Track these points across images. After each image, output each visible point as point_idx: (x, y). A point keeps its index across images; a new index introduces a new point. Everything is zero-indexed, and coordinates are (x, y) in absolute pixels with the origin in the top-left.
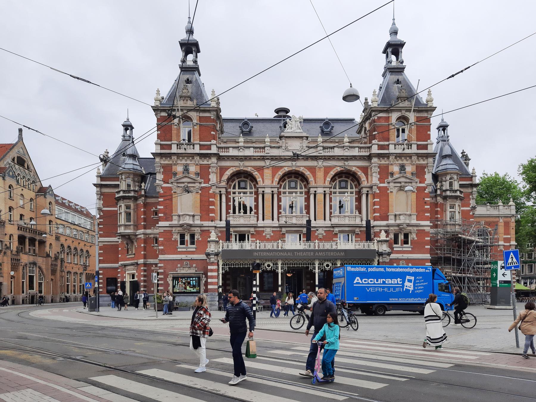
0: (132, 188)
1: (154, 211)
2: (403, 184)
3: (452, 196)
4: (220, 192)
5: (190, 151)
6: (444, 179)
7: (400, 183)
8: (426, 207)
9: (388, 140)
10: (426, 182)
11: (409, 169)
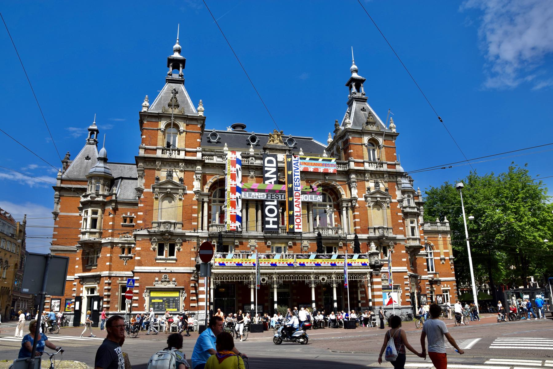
0: (101, 193)
1: (123, 217)
2: (379, 199)
4: (203, 199)
5: (175, 155)
7: (376, 198)
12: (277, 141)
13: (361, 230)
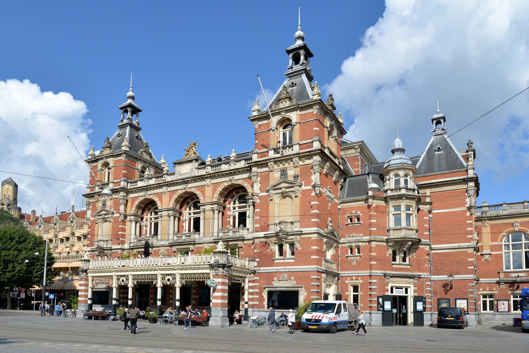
7: (280, 189)
13: (260, 228)
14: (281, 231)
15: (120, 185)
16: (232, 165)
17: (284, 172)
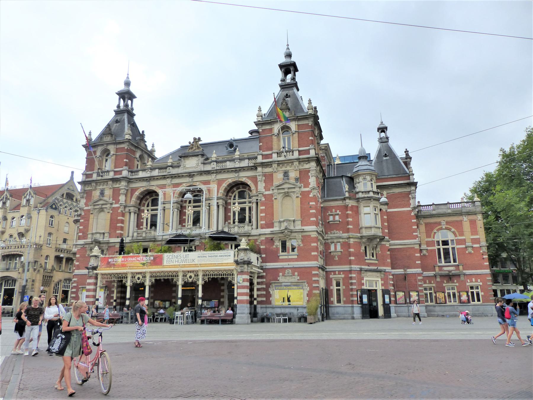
2: (286, 190)
3: (364, 198)
6: (357, 180)
7: (283, 189)
8: (311, 211)
9: (271, 149)
10: (310, 186)
11: (293, 175)
12: (195, 148)
13: (265, 224)
14: (286, 229)
15: (121, 174)
16: (237, 163)
17: (286, 174)
